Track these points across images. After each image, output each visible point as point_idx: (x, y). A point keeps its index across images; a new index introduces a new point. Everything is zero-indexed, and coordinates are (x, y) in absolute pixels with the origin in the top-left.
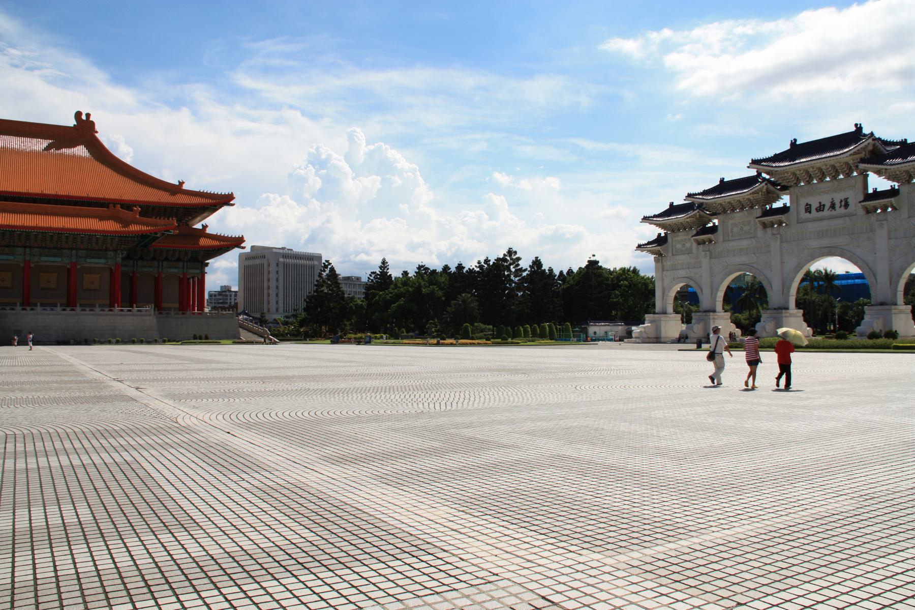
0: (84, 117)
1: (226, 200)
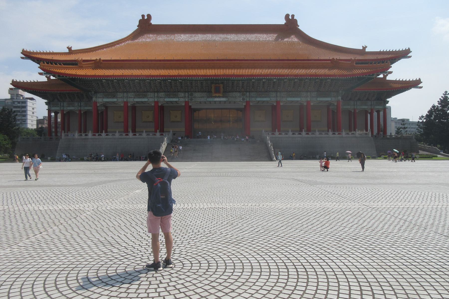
0: (290, 17)
1: (404, 54)
